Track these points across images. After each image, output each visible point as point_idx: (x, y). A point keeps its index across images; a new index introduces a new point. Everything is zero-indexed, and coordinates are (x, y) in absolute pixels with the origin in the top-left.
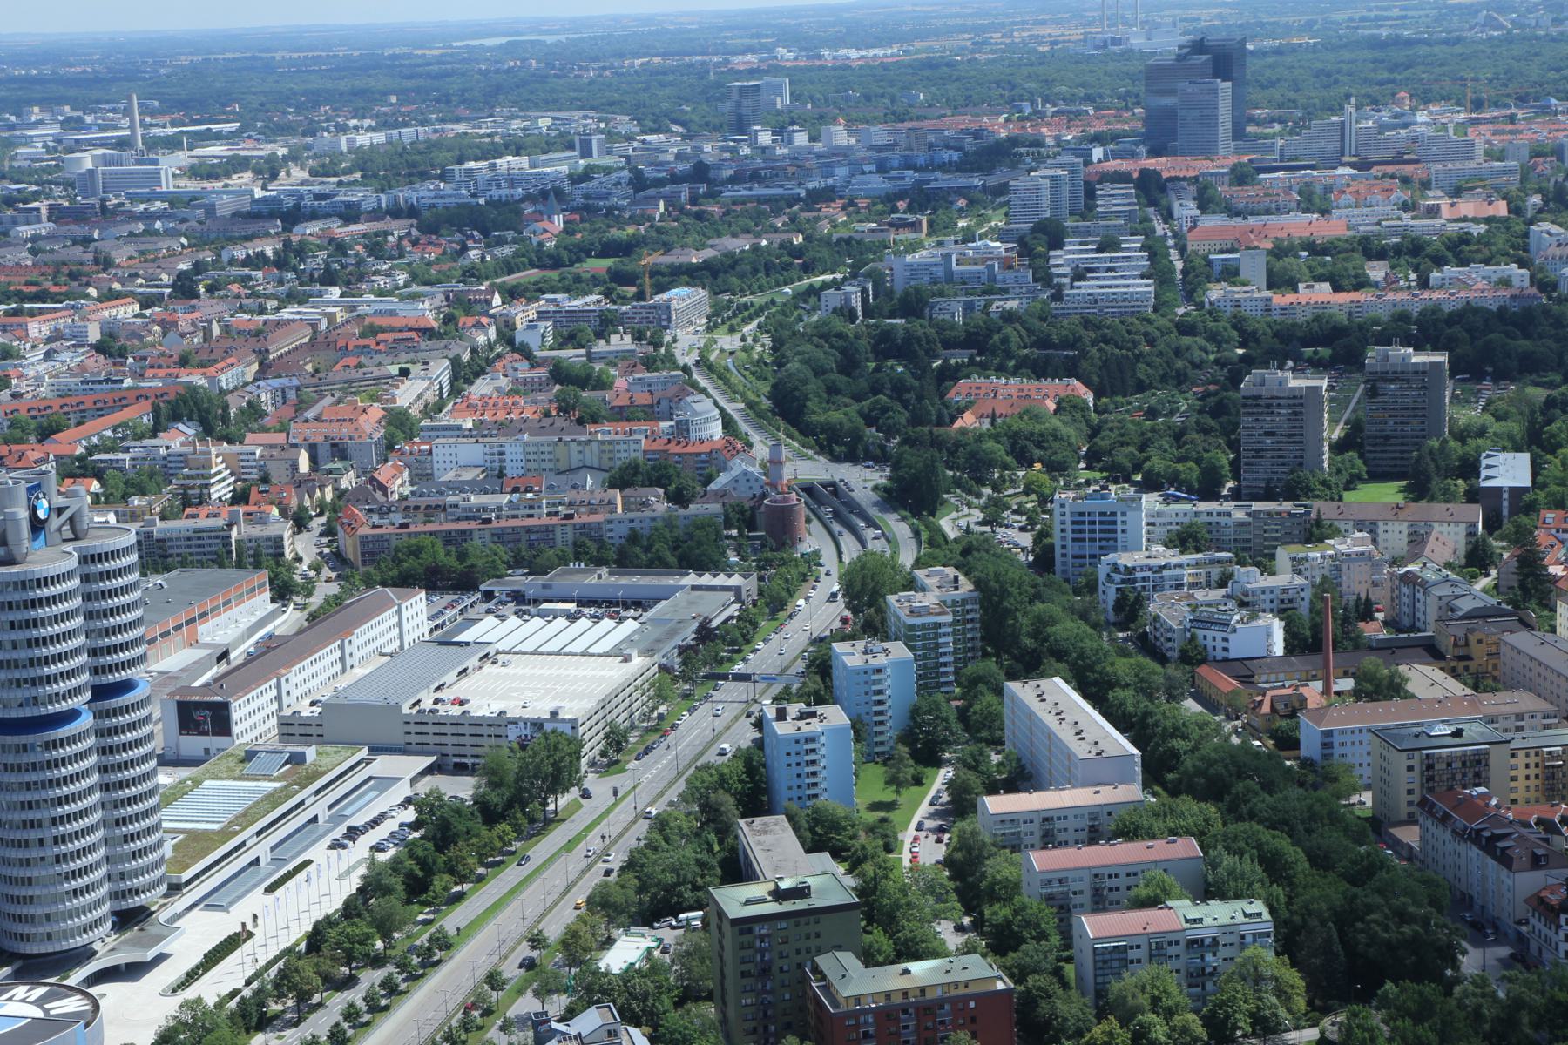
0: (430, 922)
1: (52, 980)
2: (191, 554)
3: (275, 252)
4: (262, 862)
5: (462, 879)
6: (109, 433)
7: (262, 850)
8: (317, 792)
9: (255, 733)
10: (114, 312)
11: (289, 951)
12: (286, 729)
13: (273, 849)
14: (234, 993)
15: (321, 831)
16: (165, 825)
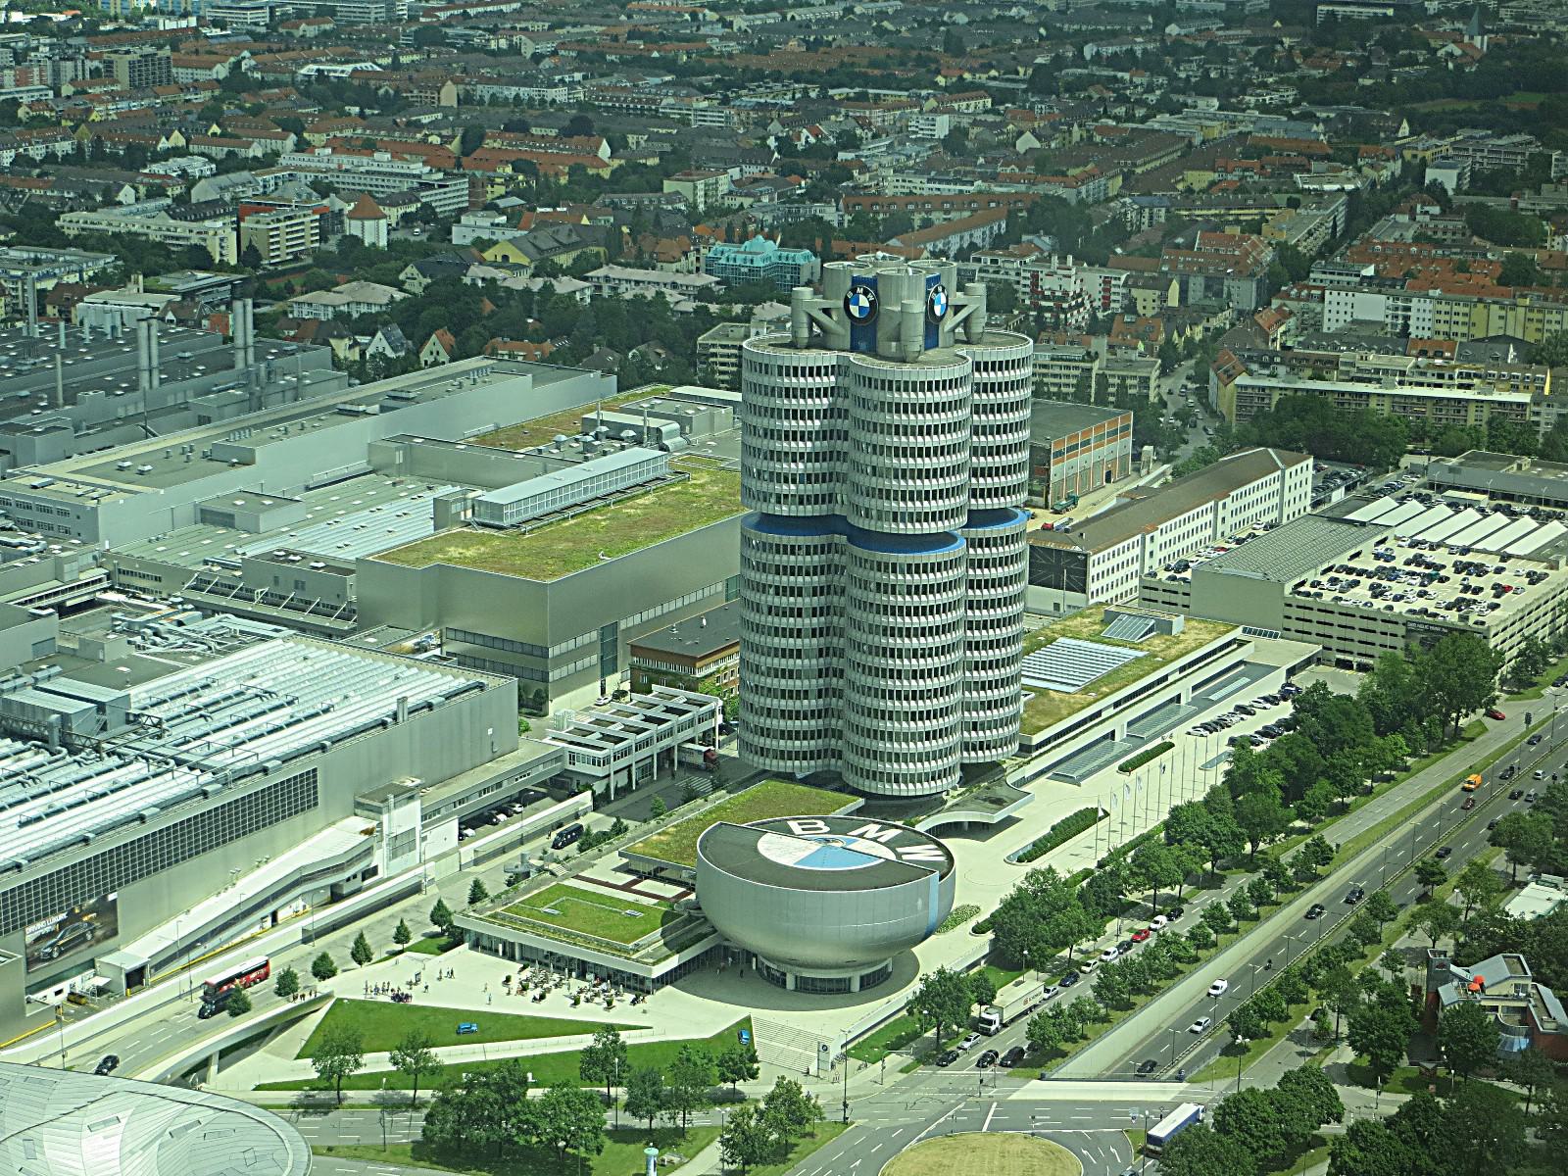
0: (1302, 831)
3: (1145, 51)
5: (1348, 792)
7: (1119, 724)
8: (1182, 669)
9: (1112, 594)
10: (964, 104)
11: (1147, 837)
12: (1148, 594)
13: (1130, 724)
14: (1087, 873)
15: (1182, 713)
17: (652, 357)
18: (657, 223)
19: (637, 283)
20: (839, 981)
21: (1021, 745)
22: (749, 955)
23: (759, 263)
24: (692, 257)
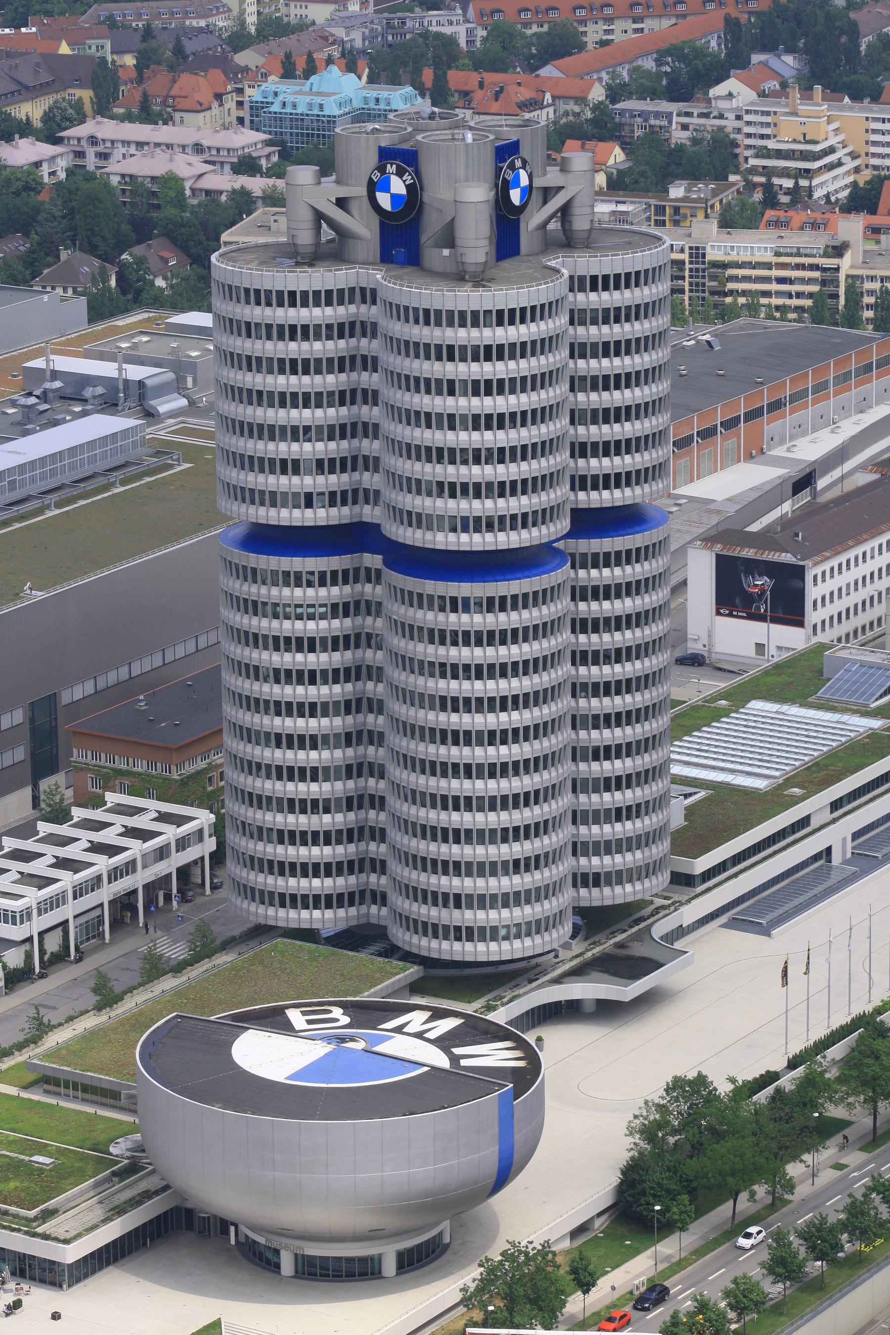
1: (469, 1008)
2: (767, 294)
4: (837, 858)
6: (649, 64)
7: (837, 836)
16: (676, 769)
17: (154, 263)
18: (179, 50)
19: (140, 145)
20: (363, 1260)
21: (673, 874)
22: (224, 1225)
23: (332, 109)
24: (230, 103)
